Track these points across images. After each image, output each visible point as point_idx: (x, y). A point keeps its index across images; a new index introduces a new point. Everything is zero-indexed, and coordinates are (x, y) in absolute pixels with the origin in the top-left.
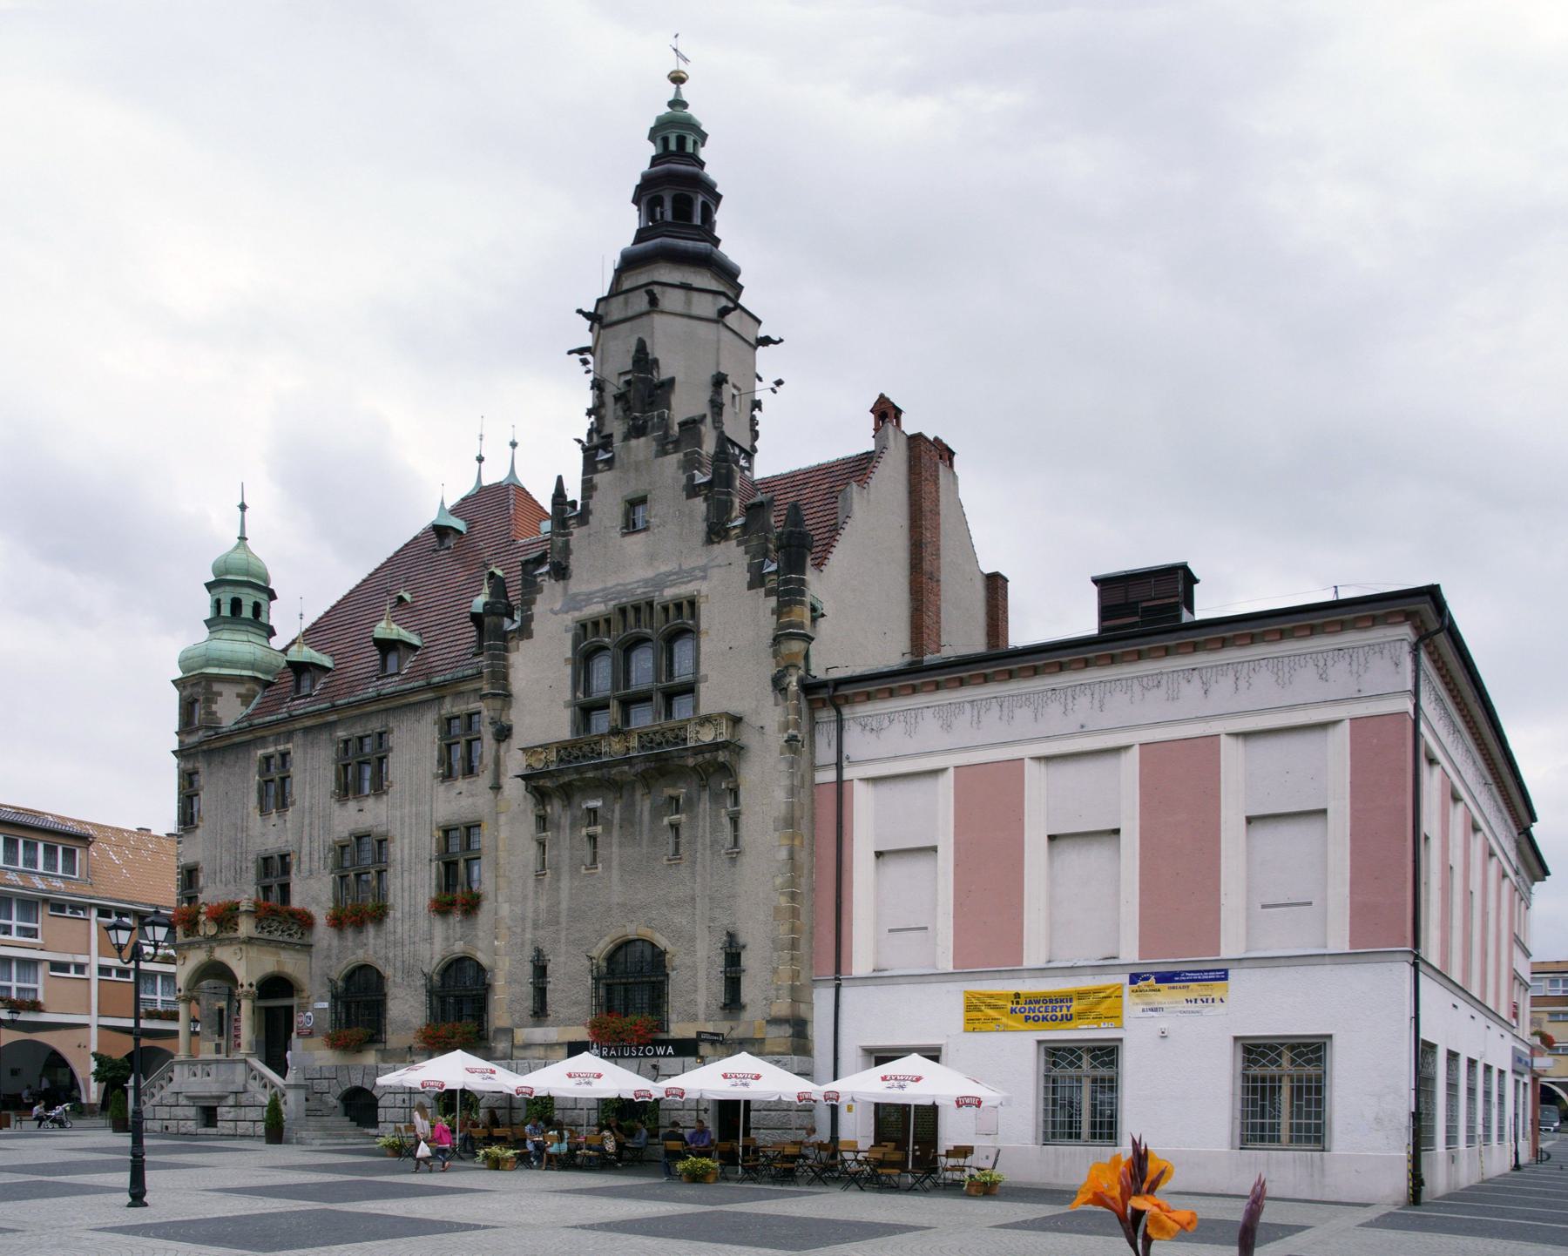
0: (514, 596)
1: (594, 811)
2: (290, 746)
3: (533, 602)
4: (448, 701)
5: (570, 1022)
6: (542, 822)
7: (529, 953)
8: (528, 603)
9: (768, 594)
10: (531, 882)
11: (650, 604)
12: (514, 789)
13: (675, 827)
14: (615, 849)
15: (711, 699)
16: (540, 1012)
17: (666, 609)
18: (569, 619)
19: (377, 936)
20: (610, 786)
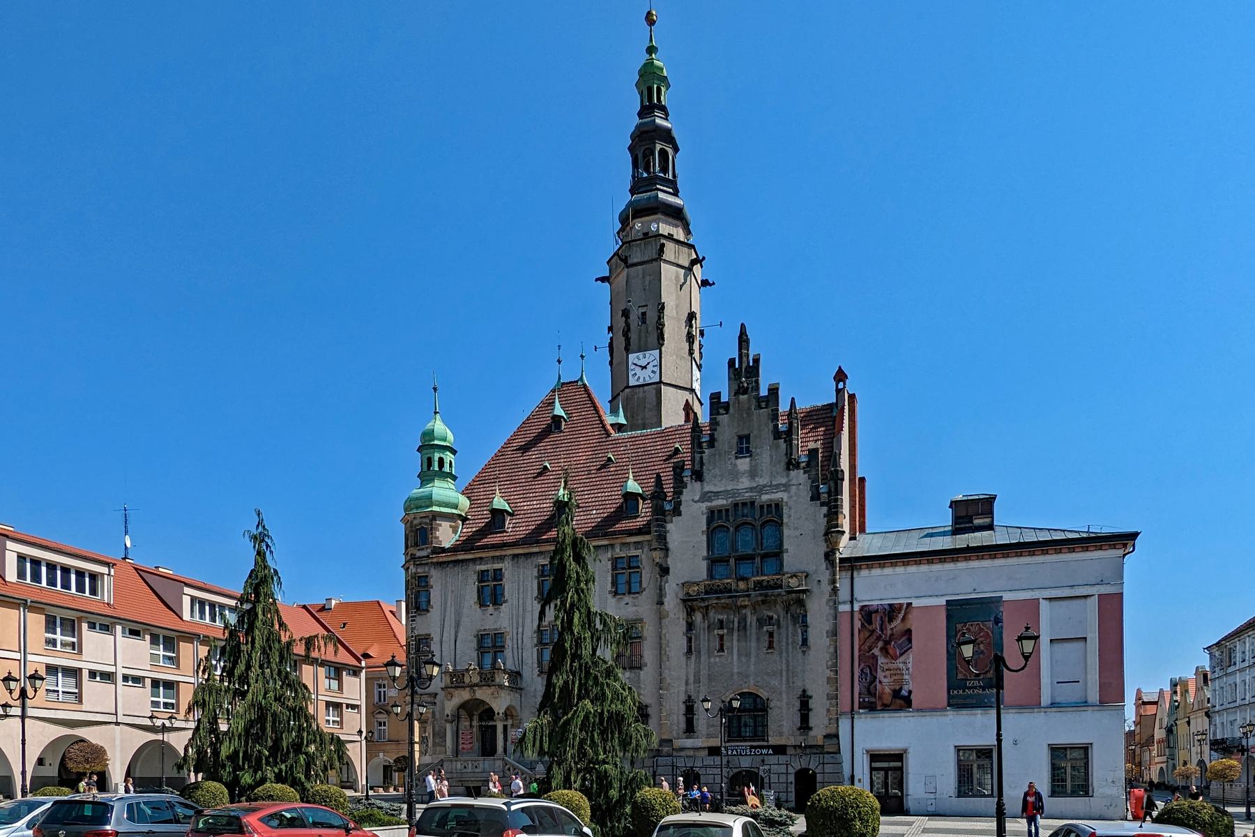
0: (669, 489)
3: (681, 493)
5: (709, 736)
7: (683, 697)
8: (678, 492)
9: (822, 504)
10: (684, 659)
11: (753, 503)
12: (672, 602)
15: (791, 561)
16: (690, 729)
17: (762, 507)
18: (704, 506)
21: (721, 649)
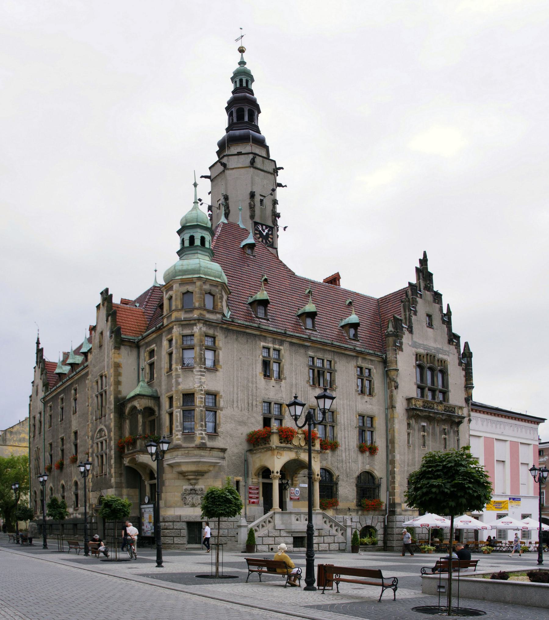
1: (424, 426)
2: (281, 347)
4: (360, 359)
6: (409, 424)
13: (445, 439)
14: (430, 442)
19: (332, 456)
20: (430, 419)
21: (424, 445)
